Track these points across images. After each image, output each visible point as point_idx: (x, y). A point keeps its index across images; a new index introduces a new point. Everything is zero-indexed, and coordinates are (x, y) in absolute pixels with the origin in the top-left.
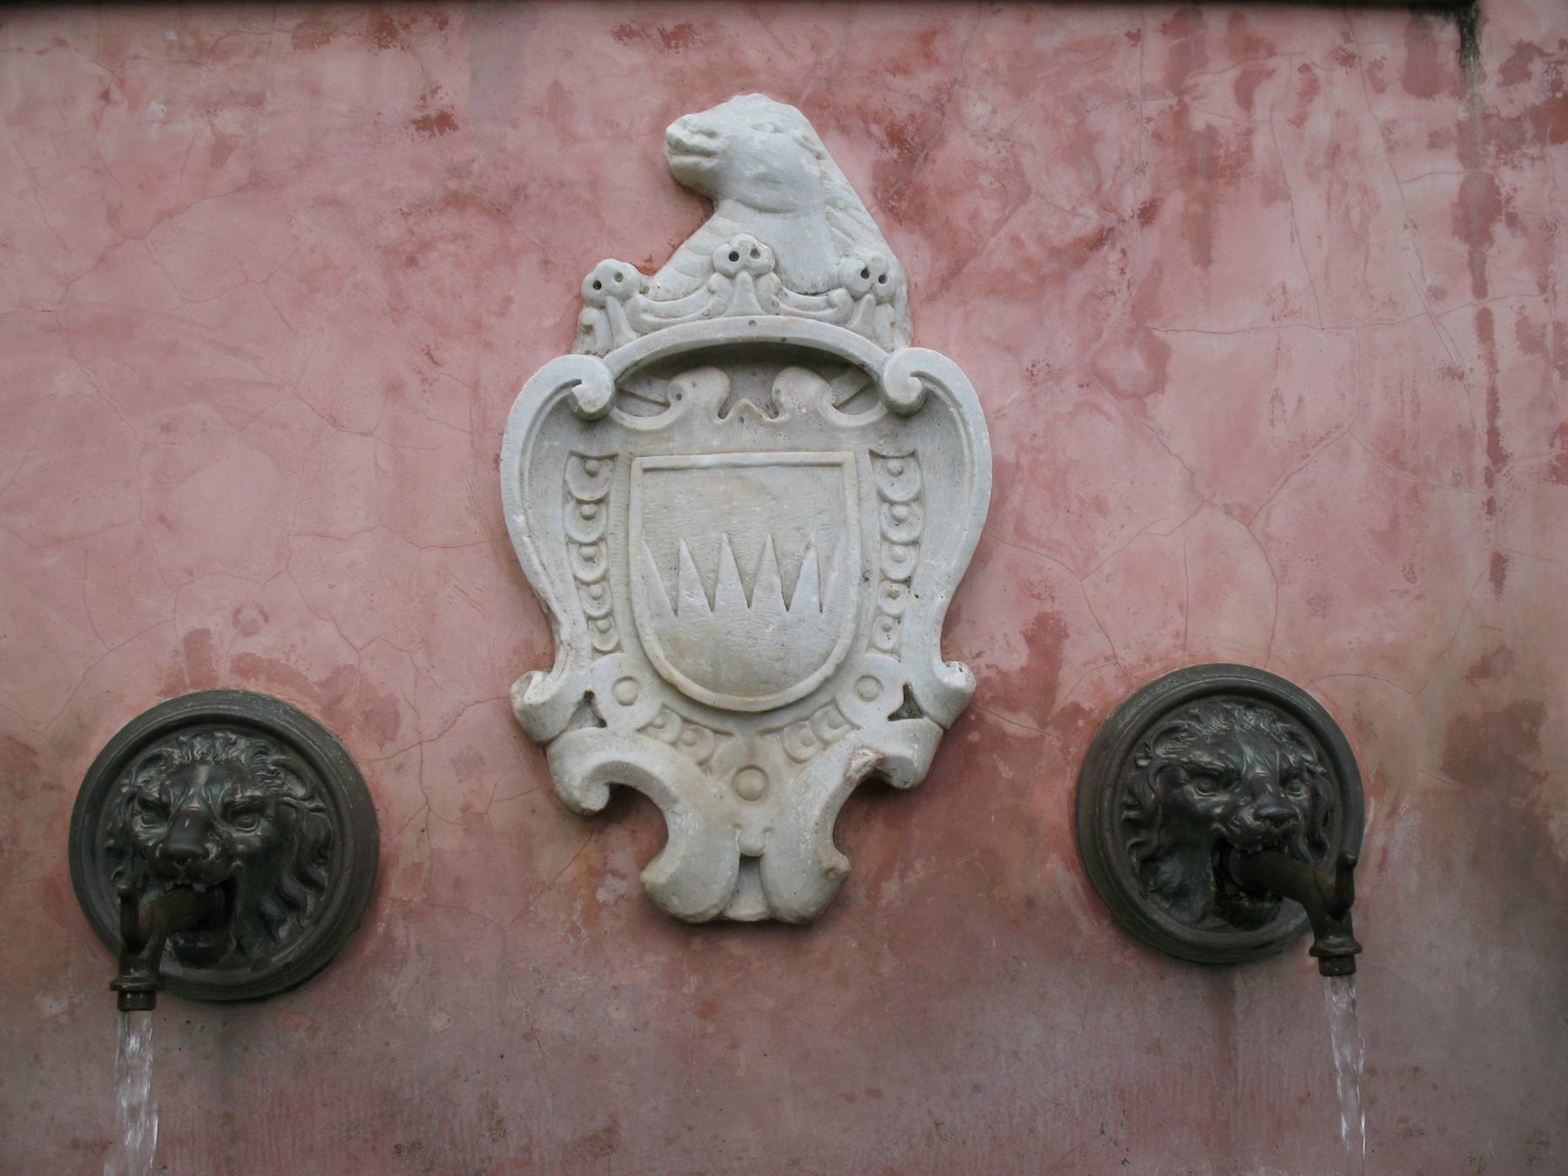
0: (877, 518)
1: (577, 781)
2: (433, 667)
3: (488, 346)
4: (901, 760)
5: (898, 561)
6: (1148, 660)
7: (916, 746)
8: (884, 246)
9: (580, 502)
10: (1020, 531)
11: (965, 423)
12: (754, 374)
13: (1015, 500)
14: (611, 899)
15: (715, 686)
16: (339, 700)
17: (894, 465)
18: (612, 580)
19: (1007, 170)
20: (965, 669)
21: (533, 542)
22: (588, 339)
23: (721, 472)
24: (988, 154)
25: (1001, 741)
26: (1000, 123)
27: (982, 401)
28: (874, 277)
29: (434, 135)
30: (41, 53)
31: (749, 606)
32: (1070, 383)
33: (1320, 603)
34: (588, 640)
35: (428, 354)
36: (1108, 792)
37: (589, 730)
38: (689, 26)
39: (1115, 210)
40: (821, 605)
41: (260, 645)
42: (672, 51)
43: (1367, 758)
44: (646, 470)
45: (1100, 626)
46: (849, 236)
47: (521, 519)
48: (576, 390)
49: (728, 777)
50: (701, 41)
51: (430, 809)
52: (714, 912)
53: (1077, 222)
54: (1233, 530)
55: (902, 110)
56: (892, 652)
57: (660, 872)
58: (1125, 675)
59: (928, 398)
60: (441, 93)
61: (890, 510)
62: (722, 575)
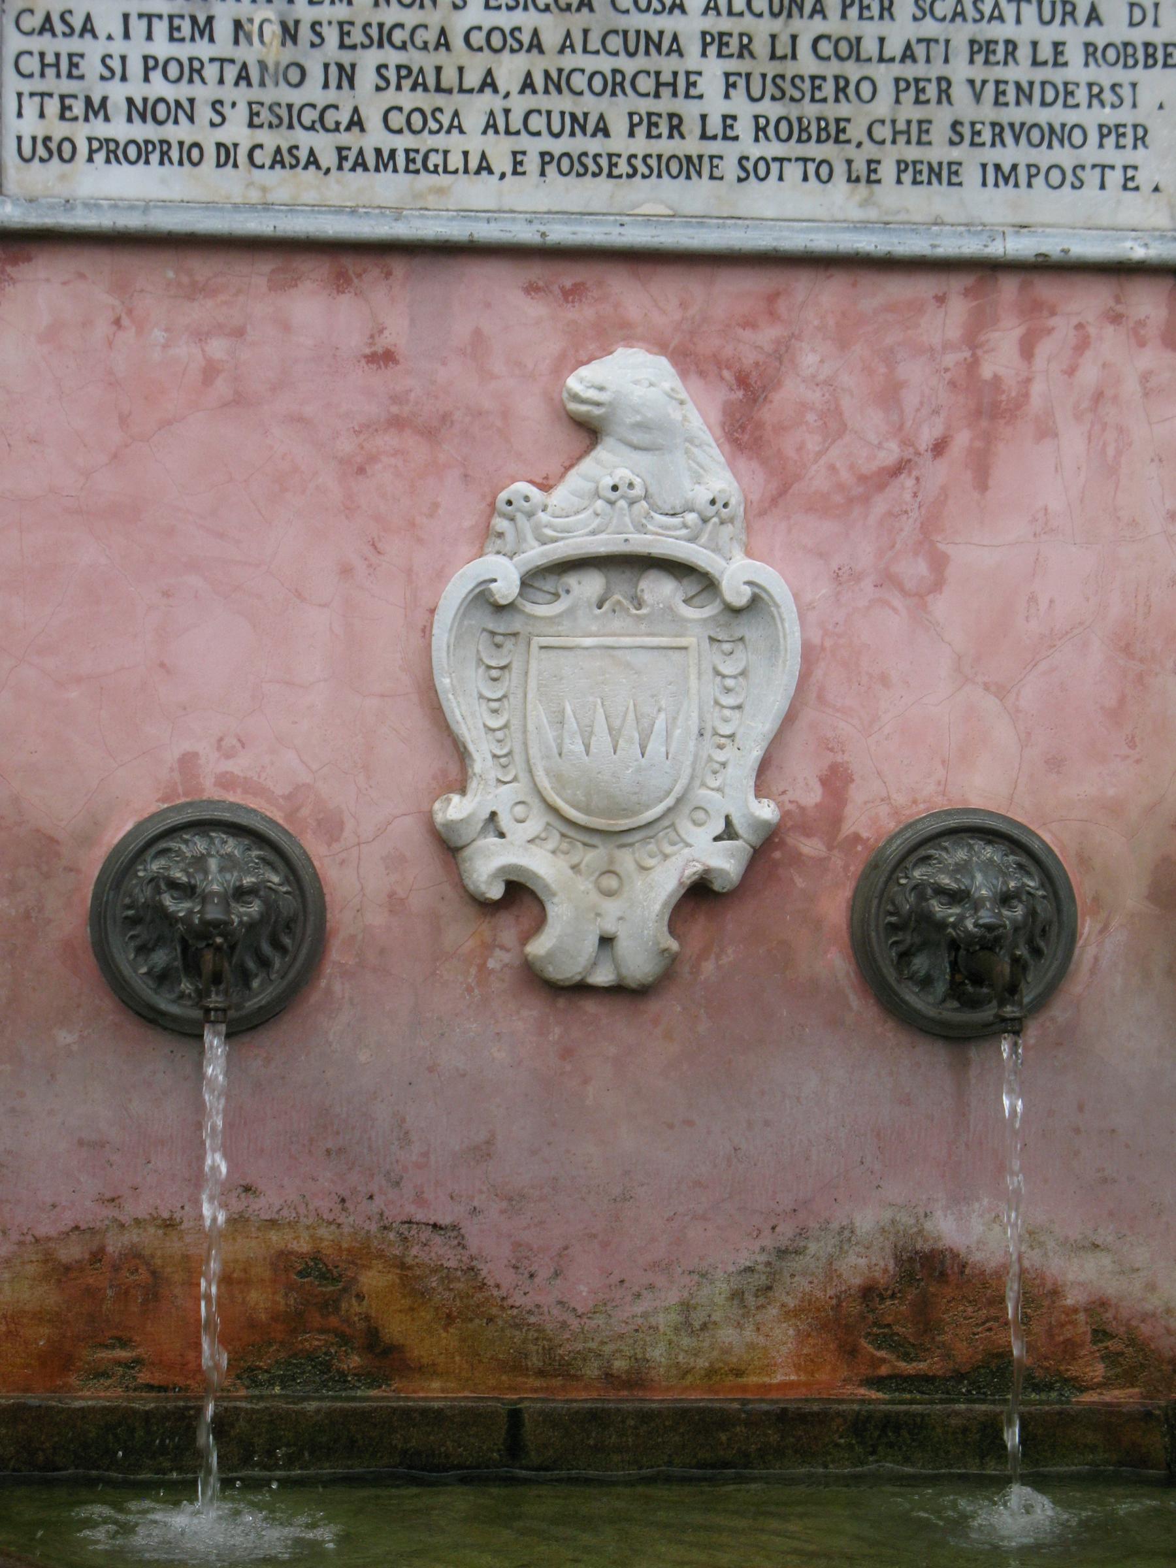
0: (712, 688)
1: (484, 878)
2: (371, 787)
3: (420, 541)
4: (721, 872)
5: (726, 720)
6: (915, 802)
7: (732, 861)
8: (728, 475)
9: (489, 667)
10: (821, 698)
11: (782, 620)
12: (623, 572)
13: (818, 673)
14: (498, 966)
15: (587, 811)
16: (298, 809)
17: (727, 647)
18: (512, 728)
19: (829, 410)
20: (773, 805)
21: (456, 698)
22: (499, 541)
23: (598, 652)
24: (815, 396)
25: (797, 859)
26: (826, 371)
27: (796, 596)
28: (719, 504)
29: (380, 367)
30: (64, 283)
31: (615, 753)
32: (867, 584)
33: (1055, 763)
34: (494, 773)
35: (373, 545)
36: (875, 902)
37: (492, 840)
38: (583, 284)
39: (912, 445)
40: (667, 754)
41: (237, 766)
42: (569, 305)
43: (1083, 887)
44: (542, 648)
45: (878, 773)
46: (702, 467)
47: (447, 681)
48: (493, 586)
49: (593, 878)
50: (593, 297)
51: (364, 895)
52: (578, 978)
53: (882, 454)
54: (990, 703)
55: (749, 358)
56: (718, 790)
57: (539, 947)
58: (897, 813)
59: (755, 600)
60: (386, 333)
61: (722, 682)
62: (596, 729)
